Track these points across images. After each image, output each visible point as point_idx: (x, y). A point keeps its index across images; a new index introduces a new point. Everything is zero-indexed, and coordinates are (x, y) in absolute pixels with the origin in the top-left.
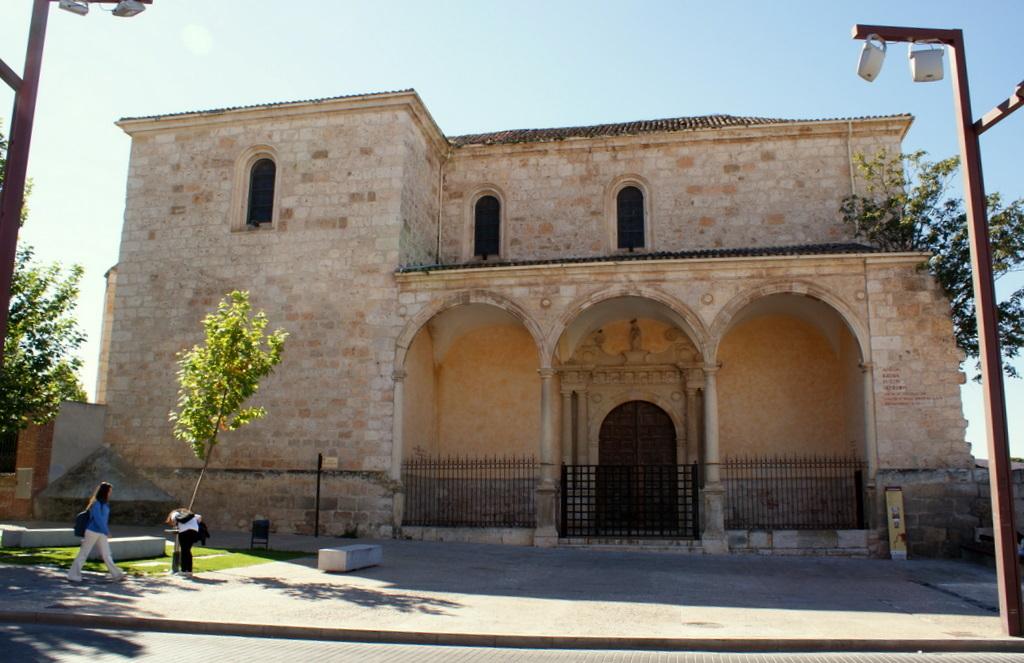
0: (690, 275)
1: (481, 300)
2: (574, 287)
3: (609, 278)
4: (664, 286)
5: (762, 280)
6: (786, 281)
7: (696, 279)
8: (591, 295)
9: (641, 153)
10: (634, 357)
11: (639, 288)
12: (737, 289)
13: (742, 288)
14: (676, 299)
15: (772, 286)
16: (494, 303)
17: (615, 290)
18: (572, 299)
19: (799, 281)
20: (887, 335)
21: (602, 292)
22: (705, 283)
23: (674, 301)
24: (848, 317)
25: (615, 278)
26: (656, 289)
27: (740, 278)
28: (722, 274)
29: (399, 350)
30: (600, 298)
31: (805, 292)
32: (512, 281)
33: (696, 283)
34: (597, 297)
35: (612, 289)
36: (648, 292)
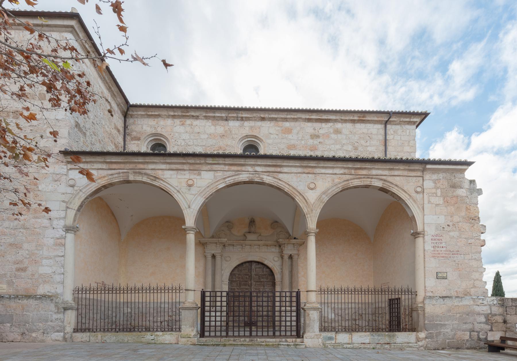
0: (300, 170)
1: (139, 178)
2: (212, 173)
3: (239, 168)
4: (281, 176)
5: (351, 177)
6: (369, 178)
7: (304, 173)
8: (225, 179)
9: (259, 123)
10: (250, 237)
11: (261, 176)
12: (333, 181)
13: (337, 181)
14: (289, 185)
15: (358, 180)
16: (149, 181)
17: (244, 177)
18: (211, 181)
19: (377, 178)
20: (436, 215)
21: (233, 178)
22: (310, 175)
23: (287, 186)
24: (409, 202)
25: (243, 168)
26: (274, 178)
27: (336, 174)
28: (323, 171)
29: (69, 210)
30: (232, 182)
31: (381, 186)
32: (163, 166)
33: (304, 175)
34: (230, 181)
35: (241, 176)
36: (268, 179)
